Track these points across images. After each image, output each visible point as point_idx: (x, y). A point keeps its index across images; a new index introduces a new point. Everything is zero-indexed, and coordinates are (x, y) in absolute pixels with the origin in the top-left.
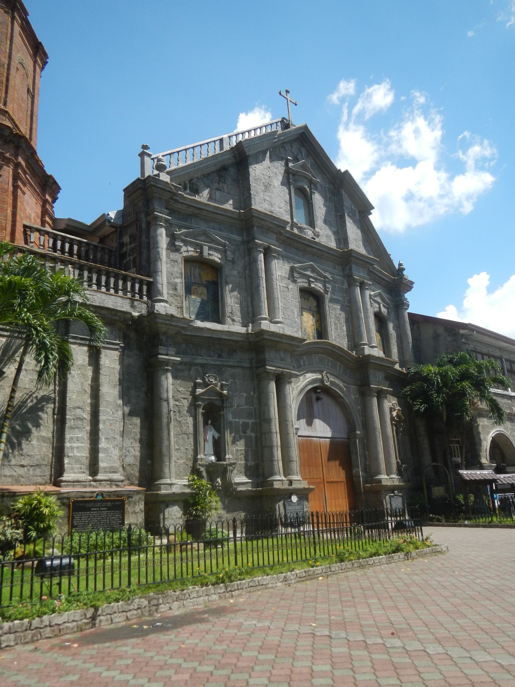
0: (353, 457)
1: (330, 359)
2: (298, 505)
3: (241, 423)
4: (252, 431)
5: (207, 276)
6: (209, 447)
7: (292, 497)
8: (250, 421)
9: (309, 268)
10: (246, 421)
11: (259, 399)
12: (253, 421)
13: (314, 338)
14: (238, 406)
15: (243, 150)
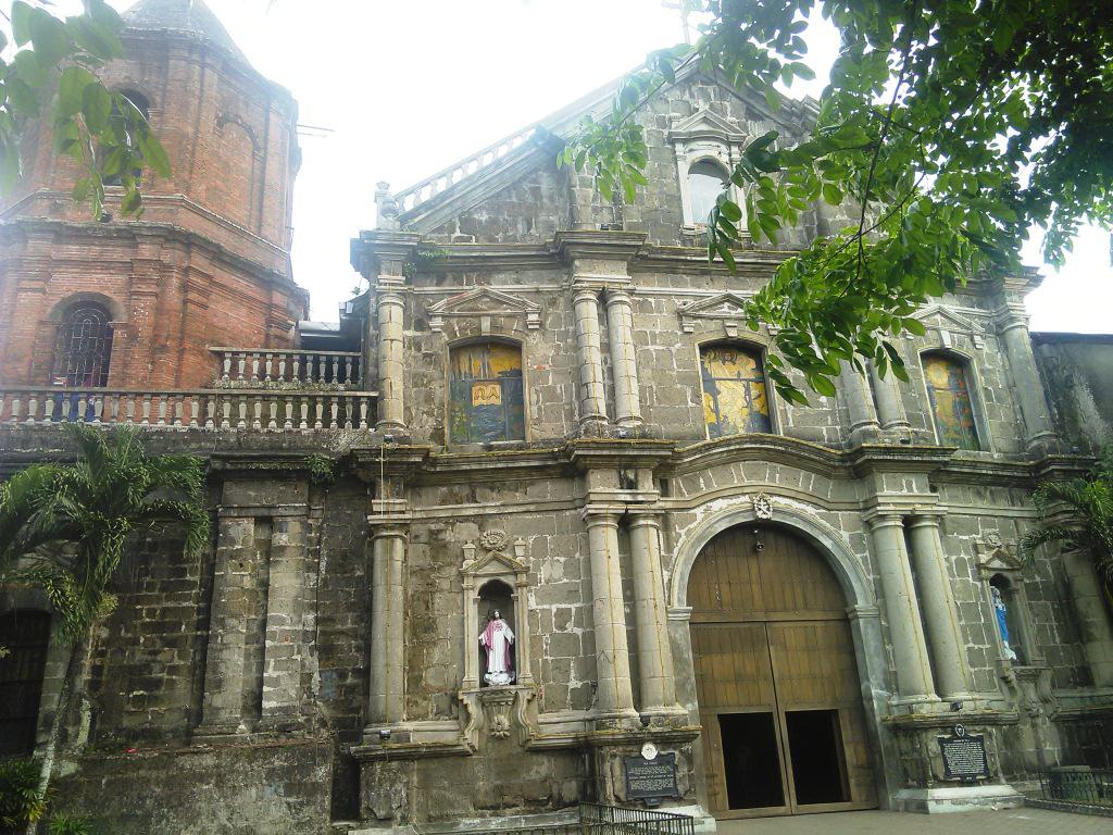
0: (858, 655)
1: (779, 466)
2: (660, 764)
3: (554, 610)
4: (577, 624)
5: (500, 364)
6: (497, 660)
7: (646, 747)
8: (573, 607)
9: (722, 303)
10: (563, 606)
11: (588, 561)
12: (578, 605)
13: (748, 429)
14: (547, 581)
15: (551, 134)
